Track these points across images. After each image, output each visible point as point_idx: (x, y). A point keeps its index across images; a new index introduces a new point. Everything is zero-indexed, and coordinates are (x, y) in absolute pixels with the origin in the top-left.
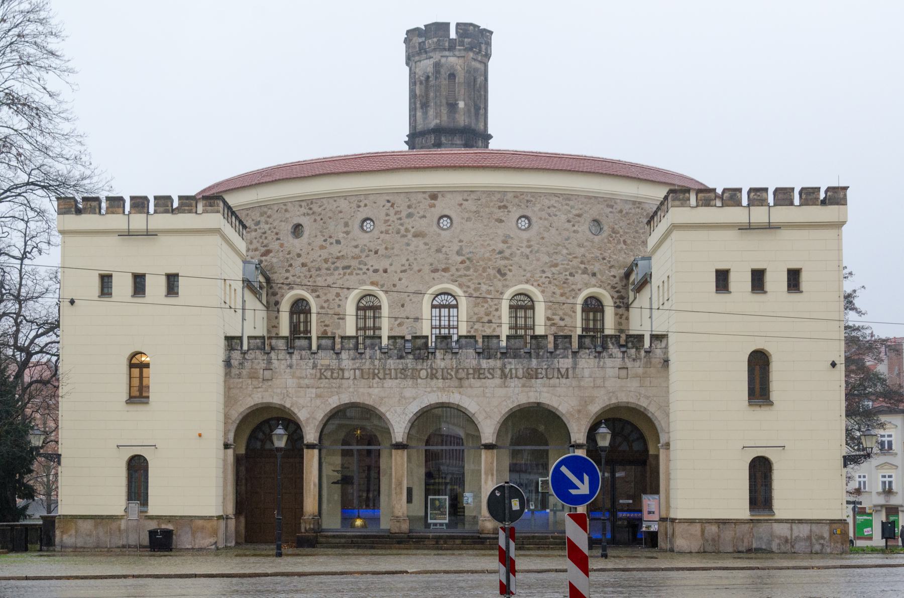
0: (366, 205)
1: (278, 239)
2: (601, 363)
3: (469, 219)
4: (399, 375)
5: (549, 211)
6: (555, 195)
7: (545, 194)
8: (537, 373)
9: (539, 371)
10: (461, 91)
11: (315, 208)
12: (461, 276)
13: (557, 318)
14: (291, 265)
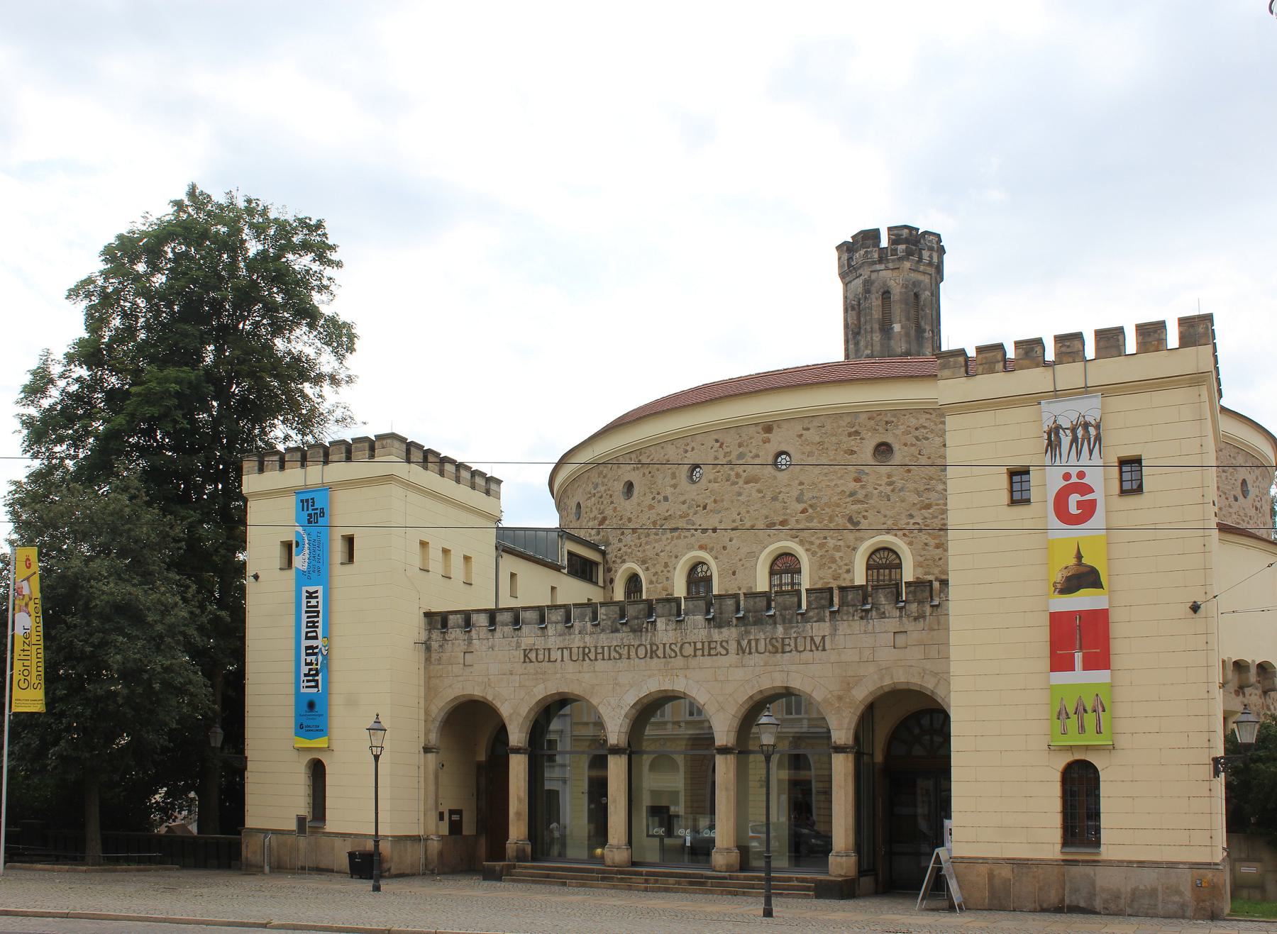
0: (693, 449)
2: (870, 627)
4: (613, 654)
5: (917, 433)
6: (926, 411)
7: (910, 412)
8: (783, 645)
9: (787, 641)
10: (897, 311)
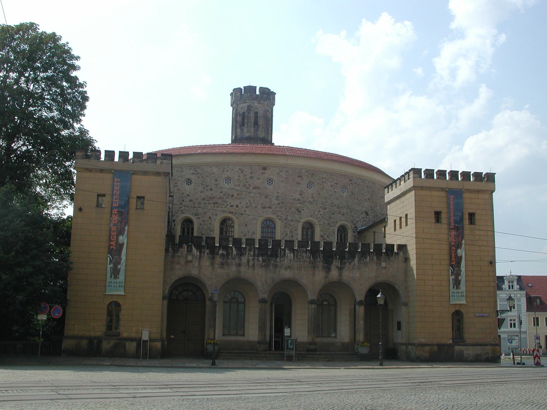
0: (227, 171)
1: (176, 186)
3: (282, 182)
5: (323, 180)
11: (199, 171)
13: (325, 237)
14: (183, 201)
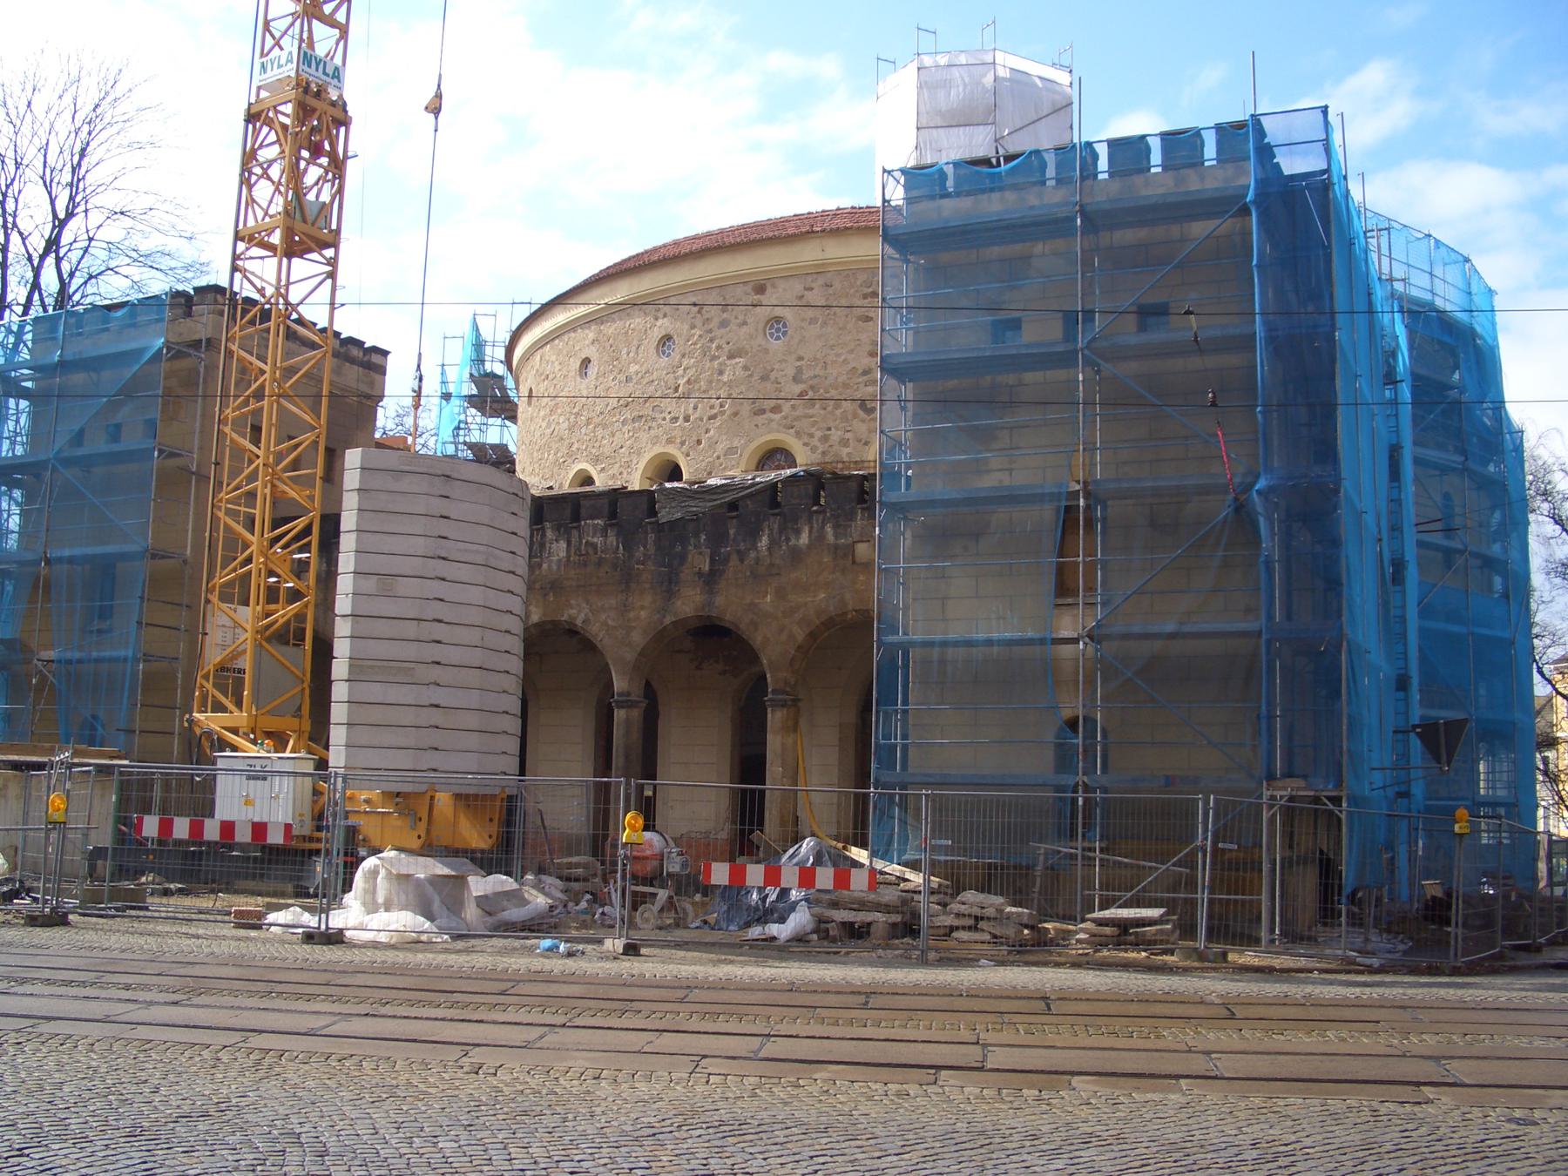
3: (813, 321)
12: (797, 418)
